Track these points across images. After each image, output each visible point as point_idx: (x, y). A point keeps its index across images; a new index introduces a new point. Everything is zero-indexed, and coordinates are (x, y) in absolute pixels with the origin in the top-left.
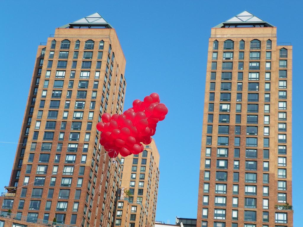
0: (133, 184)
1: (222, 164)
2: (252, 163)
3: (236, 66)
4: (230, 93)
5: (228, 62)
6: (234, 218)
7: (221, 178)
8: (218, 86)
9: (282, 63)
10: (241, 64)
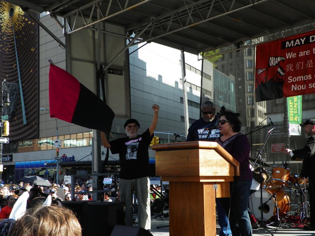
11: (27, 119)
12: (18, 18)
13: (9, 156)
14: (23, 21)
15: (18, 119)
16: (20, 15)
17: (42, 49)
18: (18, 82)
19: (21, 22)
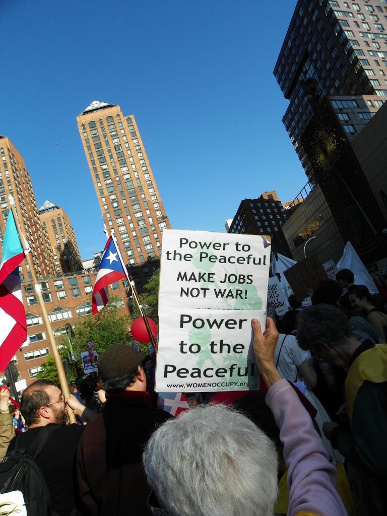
0: (58, 242)
1: (115, 205)
2: (134, 198)
3: (102, 137)
4: (104, 157)
5: (96, 137)
6: (135, 237)
7: (117, 214)
8: (95, 154)
9: (131, 128)
10: (105, 136)
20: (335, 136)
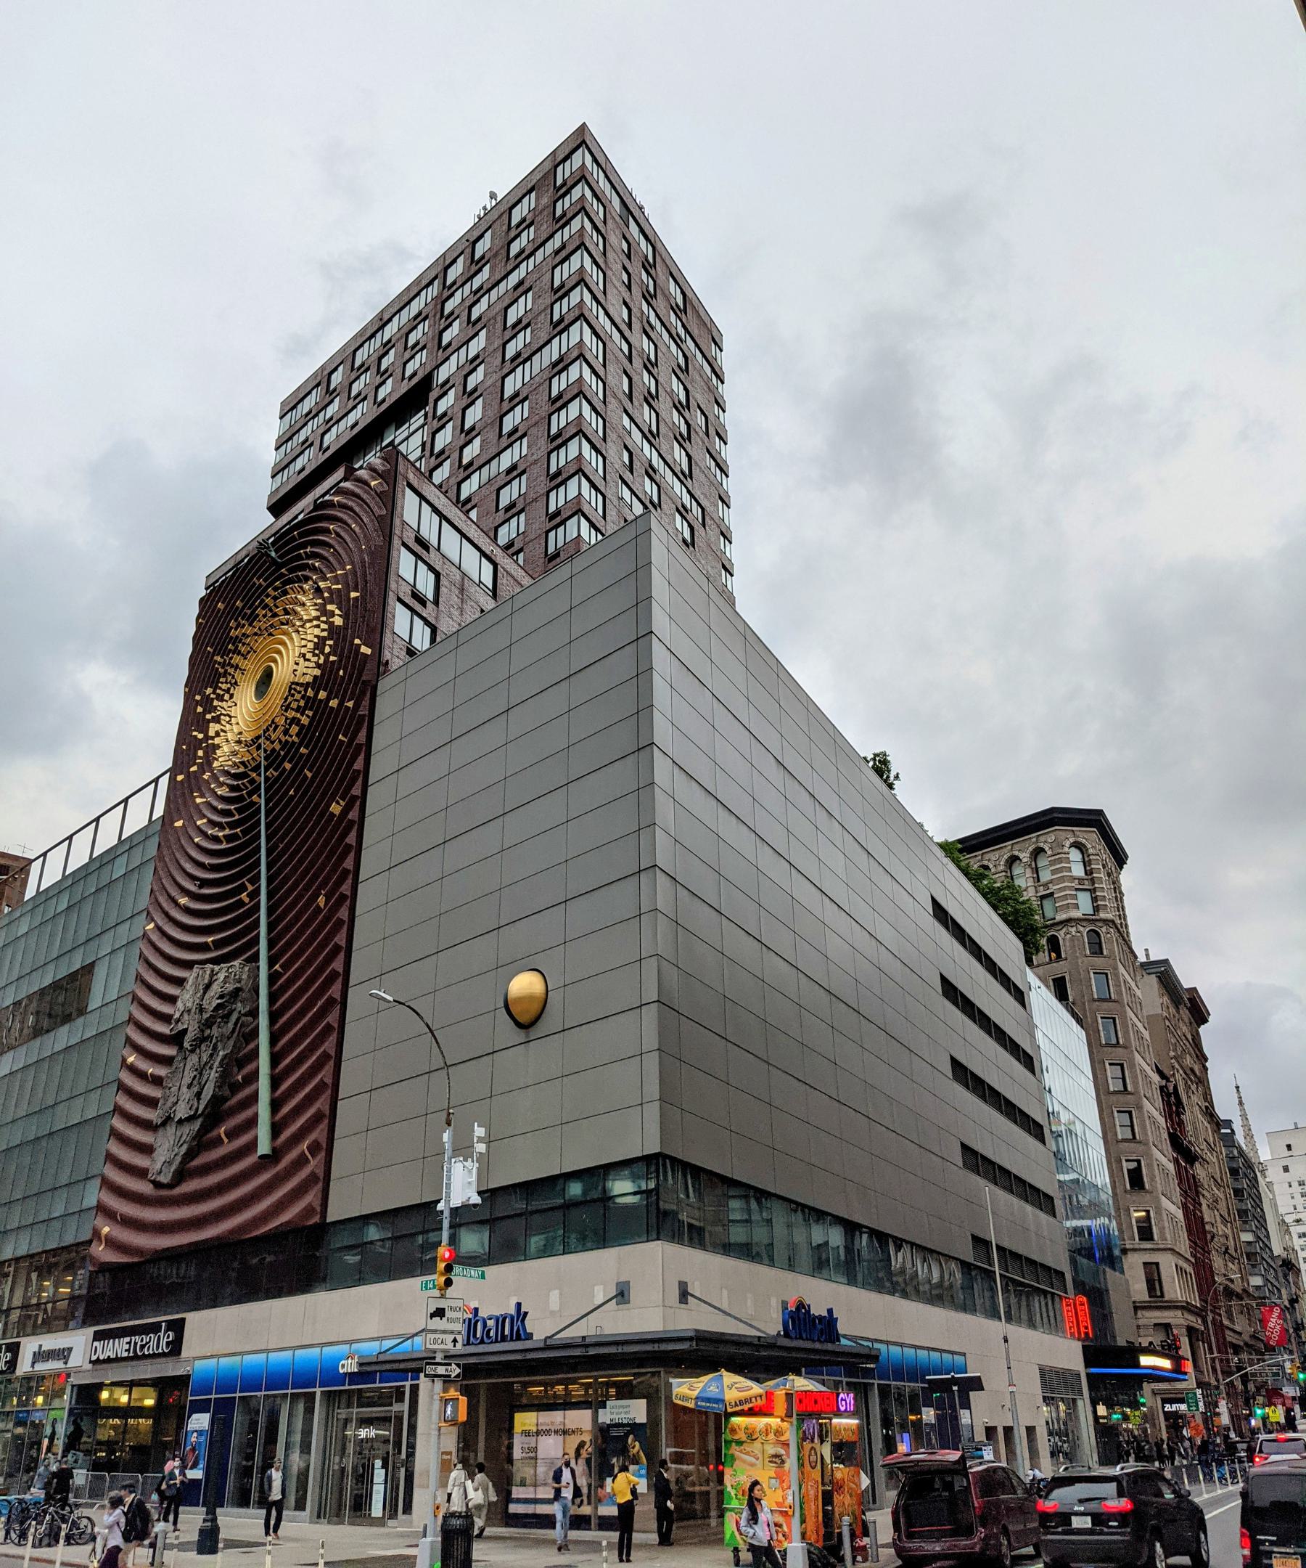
11: (276, 1130)
12: (286, 699)
13: (167, 1330)
14: (306, 704)
15: (232, 1135)
16: (297, 684)
17: (376, 797)
18: (255, 958)
19: (297, 710)
20: (338, 621)
